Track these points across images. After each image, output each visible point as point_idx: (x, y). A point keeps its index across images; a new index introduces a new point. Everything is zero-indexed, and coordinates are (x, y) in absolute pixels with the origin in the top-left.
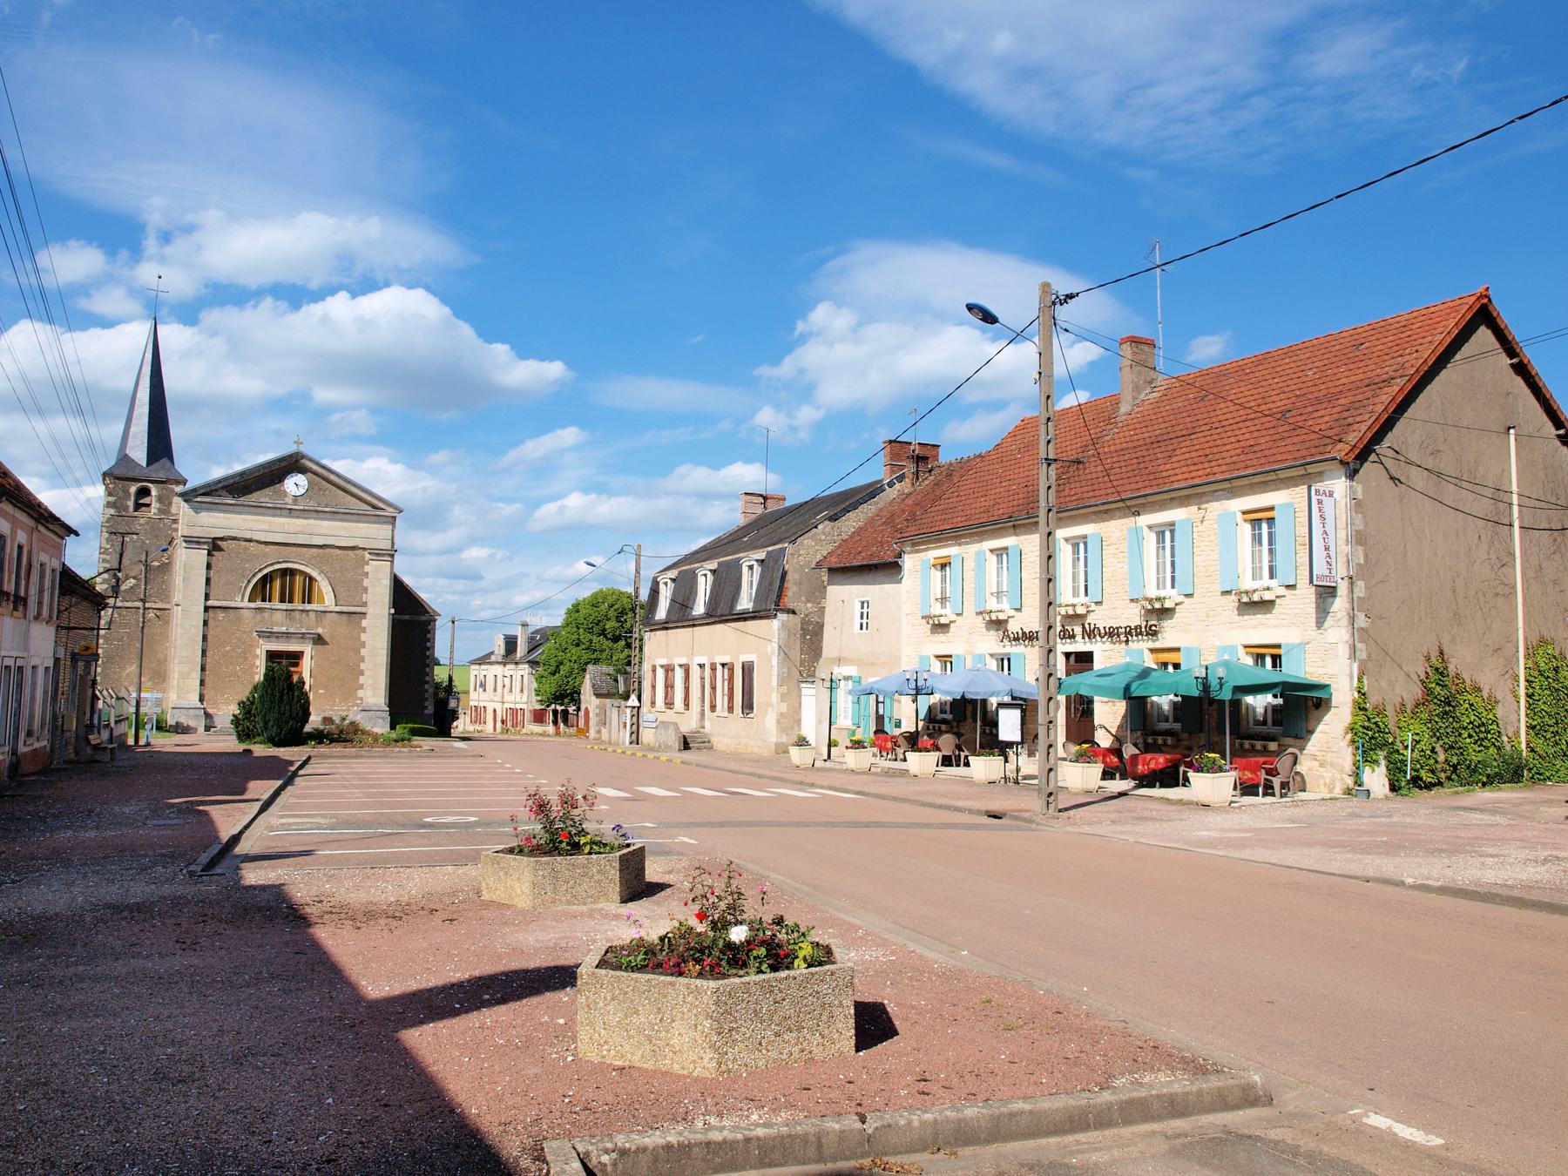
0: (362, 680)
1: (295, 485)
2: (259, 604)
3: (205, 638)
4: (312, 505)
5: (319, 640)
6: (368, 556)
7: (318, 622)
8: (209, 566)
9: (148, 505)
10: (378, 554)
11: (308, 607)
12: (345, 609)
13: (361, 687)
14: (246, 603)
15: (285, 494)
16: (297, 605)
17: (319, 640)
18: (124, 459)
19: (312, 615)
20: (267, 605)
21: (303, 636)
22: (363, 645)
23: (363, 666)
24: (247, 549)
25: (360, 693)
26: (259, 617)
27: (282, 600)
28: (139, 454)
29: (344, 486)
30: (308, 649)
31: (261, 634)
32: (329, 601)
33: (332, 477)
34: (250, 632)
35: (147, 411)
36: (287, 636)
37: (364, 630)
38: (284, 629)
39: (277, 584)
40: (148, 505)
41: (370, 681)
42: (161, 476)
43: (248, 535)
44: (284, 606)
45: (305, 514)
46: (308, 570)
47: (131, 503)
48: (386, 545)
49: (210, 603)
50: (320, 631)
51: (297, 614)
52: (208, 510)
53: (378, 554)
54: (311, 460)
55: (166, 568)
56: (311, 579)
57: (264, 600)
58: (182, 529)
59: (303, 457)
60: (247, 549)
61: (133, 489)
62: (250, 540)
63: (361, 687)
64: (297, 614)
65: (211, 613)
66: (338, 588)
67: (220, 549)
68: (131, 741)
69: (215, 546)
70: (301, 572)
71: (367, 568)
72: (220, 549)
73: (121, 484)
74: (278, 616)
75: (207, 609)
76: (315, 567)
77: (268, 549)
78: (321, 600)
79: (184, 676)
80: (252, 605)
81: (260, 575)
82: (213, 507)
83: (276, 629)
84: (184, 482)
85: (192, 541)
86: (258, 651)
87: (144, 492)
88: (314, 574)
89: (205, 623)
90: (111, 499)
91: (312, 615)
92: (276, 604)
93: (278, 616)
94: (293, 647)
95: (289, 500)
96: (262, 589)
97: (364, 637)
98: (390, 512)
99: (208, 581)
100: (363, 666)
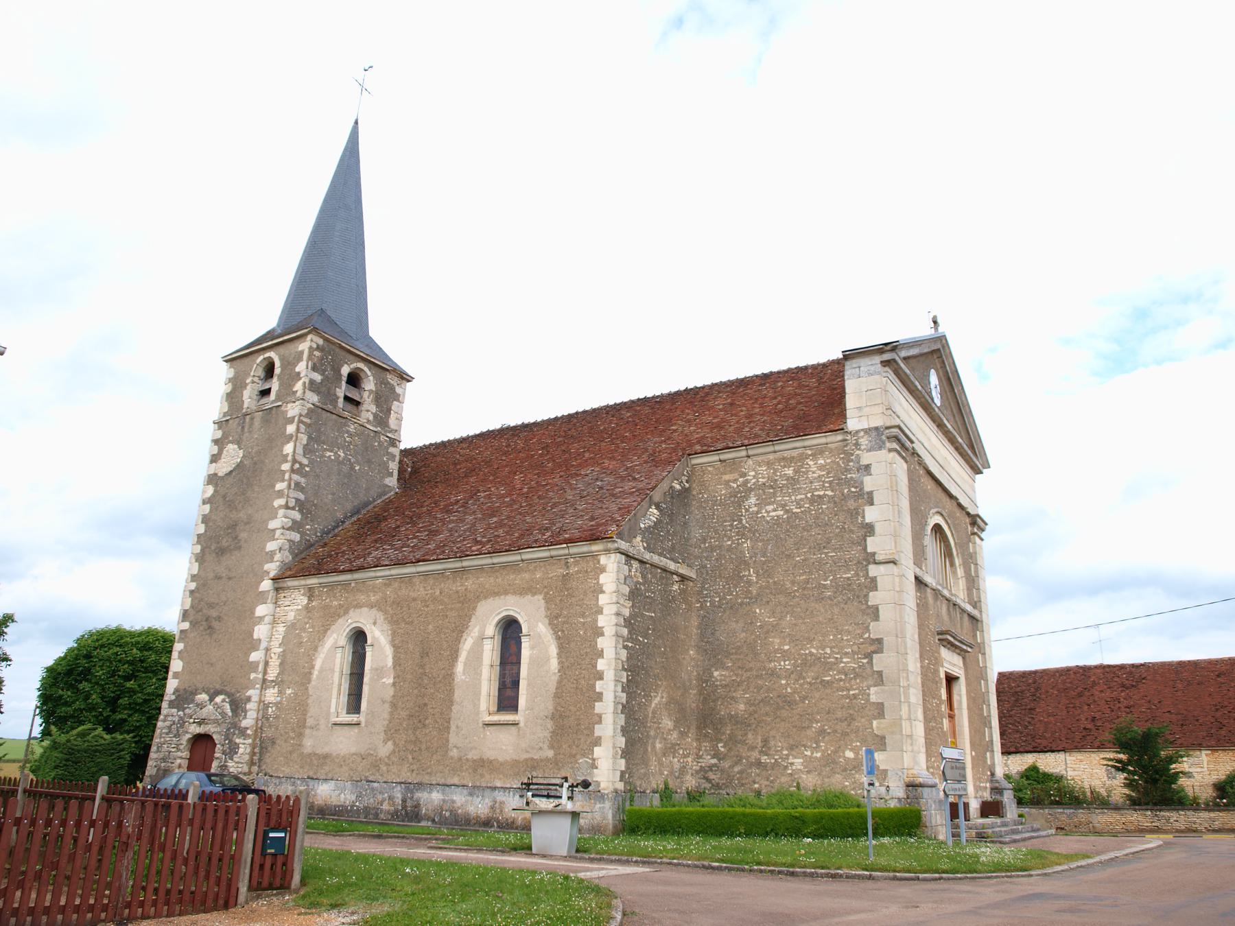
40: (357, 404)
61: (345, 370)
90: (318, 377)
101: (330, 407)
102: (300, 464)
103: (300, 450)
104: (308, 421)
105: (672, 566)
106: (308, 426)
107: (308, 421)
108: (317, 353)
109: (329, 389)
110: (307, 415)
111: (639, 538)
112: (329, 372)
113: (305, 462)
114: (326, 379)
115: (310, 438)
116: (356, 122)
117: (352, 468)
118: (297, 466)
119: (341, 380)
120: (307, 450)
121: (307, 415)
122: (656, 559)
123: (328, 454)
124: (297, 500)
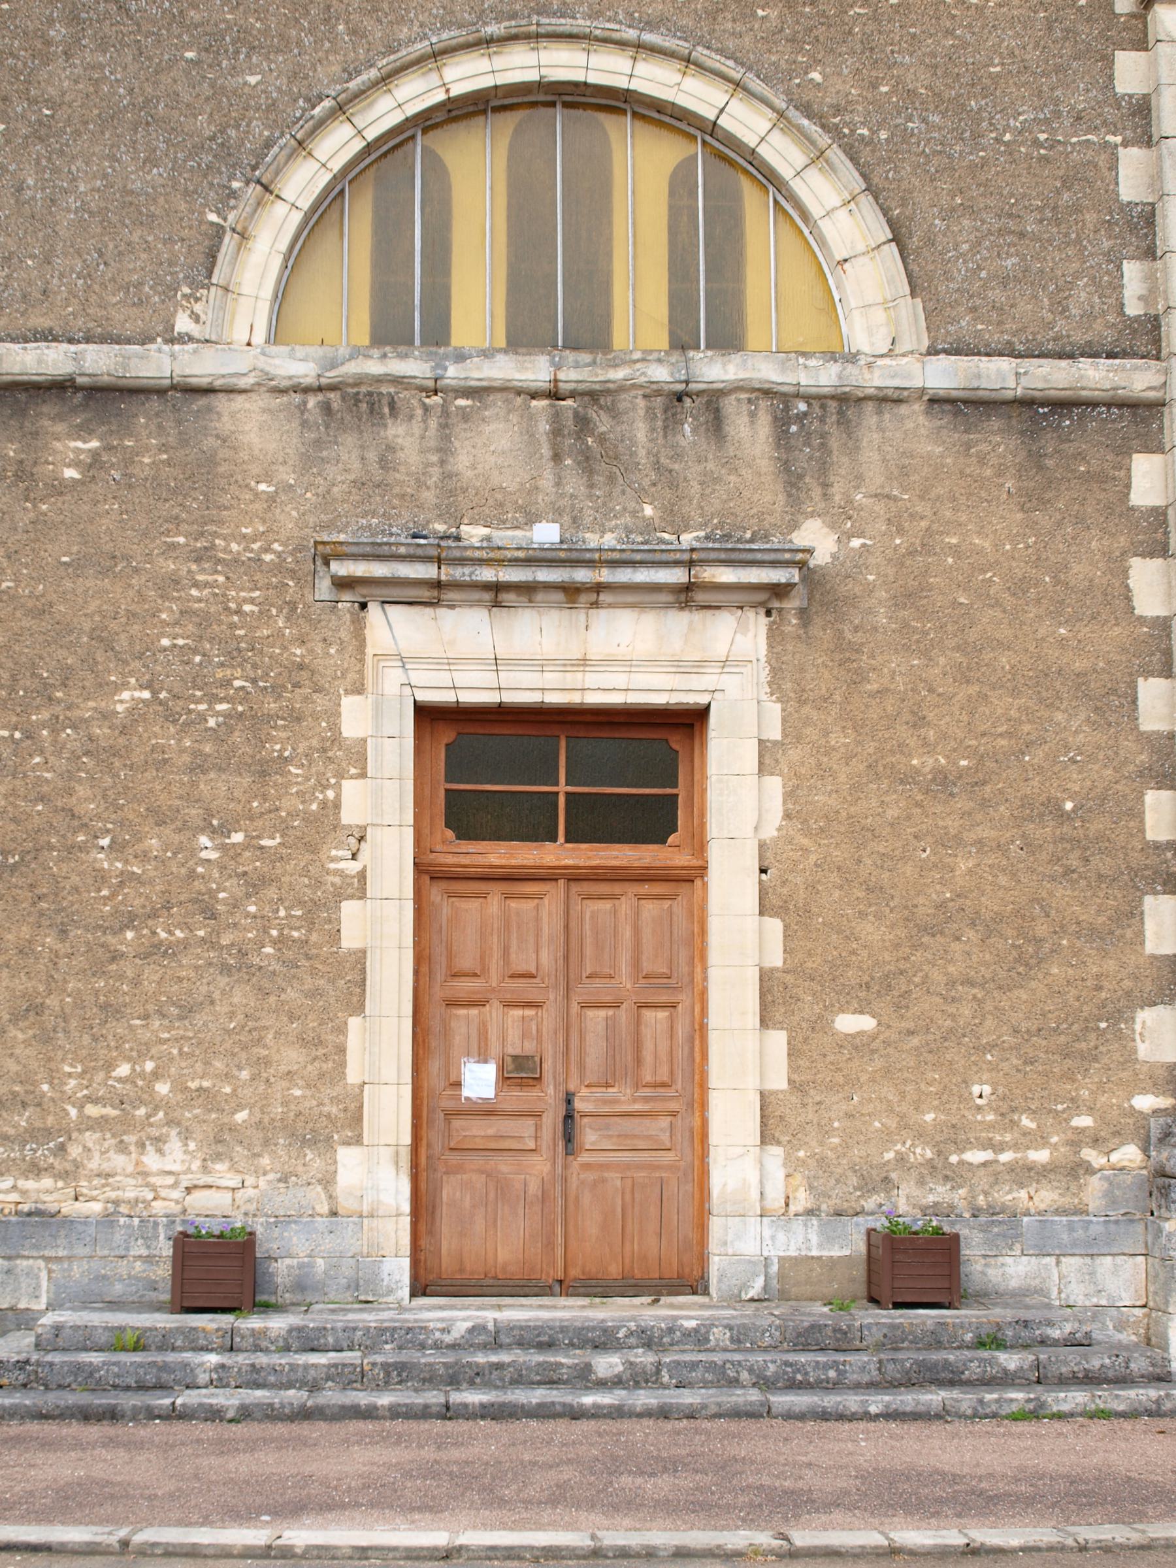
12: (998, 374)
26: (349, 456)
36: (575, 585)
38: (546, 533)
44: (537, 371)
46: (699, 95)
57: (389, 333)
71: (1130, 72)
74: (495, 450)
86: (354, 718)
91: (751, 434)
94: (618, 658)
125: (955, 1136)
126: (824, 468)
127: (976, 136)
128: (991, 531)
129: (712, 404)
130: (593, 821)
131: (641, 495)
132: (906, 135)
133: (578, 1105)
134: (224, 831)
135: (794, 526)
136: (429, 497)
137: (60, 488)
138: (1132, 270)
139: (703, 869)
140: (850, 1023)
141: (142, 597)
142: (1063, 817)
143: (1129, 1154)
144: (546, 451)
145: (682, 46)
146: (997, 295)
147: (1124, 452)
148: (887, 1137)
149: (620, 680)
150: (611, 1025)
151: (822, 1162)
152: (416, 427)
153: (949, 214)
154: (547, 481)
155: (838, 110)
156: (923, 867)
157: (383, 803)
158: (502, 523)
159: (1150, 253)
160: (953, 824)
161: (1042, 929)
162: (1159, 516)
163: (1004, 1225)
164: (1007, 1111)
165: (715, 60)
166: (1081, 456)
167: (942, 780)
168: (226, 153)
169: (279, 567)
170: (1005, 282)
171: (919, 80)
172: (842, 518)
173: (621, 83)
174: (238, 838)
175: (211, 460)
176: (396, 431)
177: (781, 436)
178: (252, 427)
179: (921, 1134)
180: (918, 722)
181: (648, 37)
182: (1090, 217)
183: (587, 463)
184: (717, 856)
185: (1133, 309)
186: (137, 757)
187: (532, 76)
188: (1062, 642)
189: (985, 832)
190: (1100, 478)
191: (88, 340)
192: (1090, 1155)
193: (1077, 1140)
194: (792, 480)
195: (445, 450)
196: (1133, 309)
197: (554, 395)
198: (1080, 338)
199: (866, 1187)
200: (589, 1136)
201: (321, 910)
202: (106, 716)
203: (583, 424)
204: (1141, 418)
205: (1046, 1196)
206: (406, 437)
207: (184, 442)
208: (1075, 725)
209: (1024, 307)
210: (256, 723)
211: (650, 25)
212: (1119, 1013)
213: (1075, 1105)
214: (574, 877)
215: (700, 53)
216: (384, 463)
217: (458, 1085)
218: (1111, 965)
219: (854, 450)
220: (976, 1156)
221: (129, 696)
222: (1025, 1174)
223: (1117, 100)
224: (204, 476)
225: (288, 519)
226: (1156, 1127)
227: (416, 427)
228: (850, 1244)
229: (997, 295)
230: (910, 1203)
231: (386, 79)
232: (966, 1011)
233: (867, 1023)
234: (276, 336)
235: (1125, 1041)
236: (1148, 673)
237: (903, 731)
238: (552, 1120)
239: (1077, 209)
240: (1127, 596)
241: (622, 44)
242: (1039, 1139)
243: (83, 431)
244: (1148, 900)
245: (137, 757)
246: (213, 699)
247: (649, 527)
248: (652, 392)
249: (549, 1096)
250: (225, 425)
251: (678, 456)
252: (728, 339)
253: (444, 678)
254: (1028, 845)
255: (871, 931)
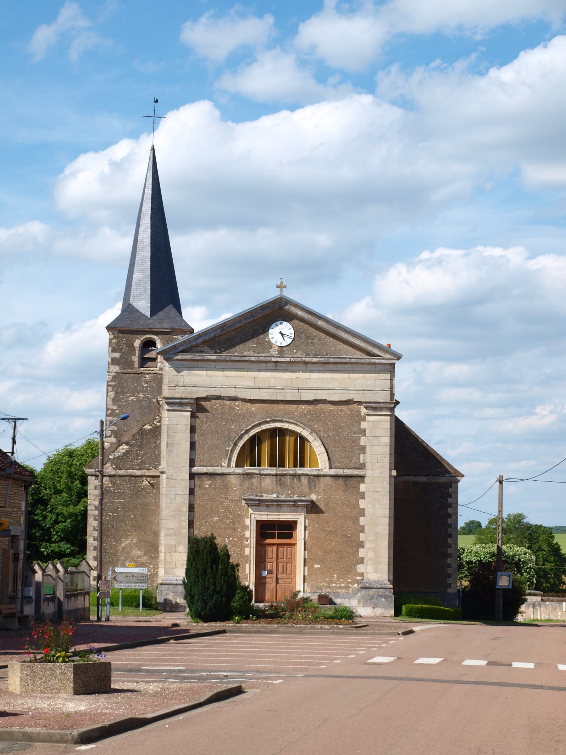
0: (362, 553)
1: (280, 334)
2: (248, 469)
3: (191, 508)
4: (299, 356)
5: (313, 508)
6: (364, 411)
7: (311, 488)
8: (193, 430)
9: (154, 360)
10: (375, 408)
11: (299, 471)
12: (340, 472)
13: (362, 561)
14: (233, 469)
15: (270, 345)
16: (289, 469)
17: (313, 508)
18: (128, 309)
19: (304, 480)
20: (255, 470)
21: (295, 505)
22: (362, 513)
23: (362, 537)
24: (231, 408)
25: (360, 568)
26: (247, 484)
27: (272, 464)
28: (143, 304)
29: (335, 333)
30: (301, 519)
31: (251, 503)
32: (322, 463)
33: (320, 323)
34: (239, 501)
35: (148, 254)
36: (278, 504)
37: (363, 496)
38: (274, 496)
39: (266, 446)
41: (371, 554)
42: (166, 326)
43: (232, 393)
44: (273, 471)
45: (292, 366)
46: (298, 429)
47: (136, 359)
48: (384, 397)
49: (195, 469)
50: (314, 497)
51: (288, 480)
52: (189, 368)
53: (375, 408)
54: (296, 305)
55: (157, 430)
56: (303, 440)
57: (252, 465)
58: (166, 392)
59: (288, 302)
60: (231, 408)
61: (137, 343)
62: (235, 399)
63: (362, 561)
64: (288, 480)
65: (197, 481)
66: (331, 449)
67: (204, 410)
68: (93, 617)
69: (198, 406)
70: (292, 433)
71: (363, 425)
72: (204, 410)
73: (125, 338)
74: (268, 482)
75: (192, 476)
76: (306, 425)
77: (254, 408)
78: (314, 463)
79: (172, 549)
80: (239, 470)
81: (246, 438)
82: (193, 365)
83: (265, 497)
84: (192, 331)
85: (176, 403)
86: (247, 522)
87: (149, 345)
88: (305, 433)
89: (192, 492)
90: (117, 355)
91: (304, 480)
92: (266, 469)
93: (268, 482)
95: (274, 352)
96: (250, 454)
97: (362, 504)
98: (386, 358)
99: (193, 446)
100: (362, 537)
101: (129, 370)
102: (112, 410)
103: (110, 402)
104: (114, 383)
105: (139, 473)
106: (113, 386)
107: (114, 383)
108: (114, 341)
109: (126, 360)
110: (112, 381)
111: (108, 464)
112: (125, 349)
113: (115, 408)
114: (123, 354)
115: (117, 393)
116: (153, 149)
117: (151, 402)
118: (110, 411)
119: (135, 350)
120: (115, 401)
121: (112, 381)
122: (122, 472)
123: (131, 398)
124: (112, 431)
125: (331, 582)
126: (315, 486)
127: (340, 435)
128: (339, 494)
129: (299, 475)
130: (280, 537)
131: (288, 490)
132: (329, 435)
133: (278, 577)
134: (229, 538)
135: (310, 494)
136: (258, 490)
137: (206, 488)
138: (362, 456)
139: (296, 544)
140: (317, 566)
141: (217, 504)
142: (348, 537)
143: (356, 585)
144: (275, 483)
145: (295, 422)
146: (341, 460)
147: (359, 483)
148: (321, 582)
149: (285, 517)
150: (283, 565)
151: (312, 585)
152: (256, 480)
153: (335, 447)
154: (275, 488)
155: (319, 431)
156: (327, 544)
157: (251, 534)
158: (268, 494)
159: (365, 453)
160: (332, 538)
161: (344, 553)
162: (364, 493)
163: (338, 595)
164: (338, 579)
165: (301, 425)
166: (353, 484)
167: (330, 531)
168: (229, 439)
169: (237, 500)
170: (343, 458)
171: (331, 427)
172: (317, 493)
173: (287, 427)
174: (231, 539)
175: (227, 484)
176: (253, 480)
177: (309, 481)
178: (233, 480)
179: (326, 582)
180: (327, 523)
181: (291, 421)
182: (356, 448)
183: (281, 485)
184: (298, 542)
185: (362, 462)
186: (217, 527)
187: (274, 426)
188: (349, 512)
189: (337, 539)
190: (355, 487)
191: (209, 466)
192: (350, 585)
193: (348, 583)
194: (310, 488)
195: (260, 483)
196: (362, 462)
197: (276, 475)
198: (354, 466)
199: (318, 589)
200: (280, 581)
201: (243, 548)
202: (213, 521)
203: (280, 479)
204: (363, 477)
205: (344, 591)
206: (255, 481)
207: (223, 482)
208: (350, 523)
209: (346, 462)
210: (233, 523)
211: (291, 418)
212: (355, 565)
213: (348, 578)
214: (278, 545)
215: (298, 423)
216: (252, 485)
217: (261, 574)
218: (354, 559)
219: (319, 483)
220: (334, 585)
221: (216, 518)
222: (340, 588)
223: (361, 429)
224: (226, 487)
225: (238, 492)
226: (359, 581)
227: (256, 480)
228: (317, 597)
229: (341, 460)
230: (323, 592)
231: (253, 428)
232: (333, 565)
233: (319, 566)
234: (236, 466)
235: (356, 570)
236: (361, 516)
237: (325, 525)
238: (274, 579)
239: (354, 446)
240: (359, 505)
241: (287, 422)
242: (343, 583)
243: (209, 480)
244: (360, 549)
245: (217, 527)
246: (227, 519)
247: (289, 494)
248: (291, 475)
249: (274, 575)
250: (229, 479)
251: (294, 484)
252: (302, 465)
253: (260, 517)
254: (343, 541)
255: (320, 553)
